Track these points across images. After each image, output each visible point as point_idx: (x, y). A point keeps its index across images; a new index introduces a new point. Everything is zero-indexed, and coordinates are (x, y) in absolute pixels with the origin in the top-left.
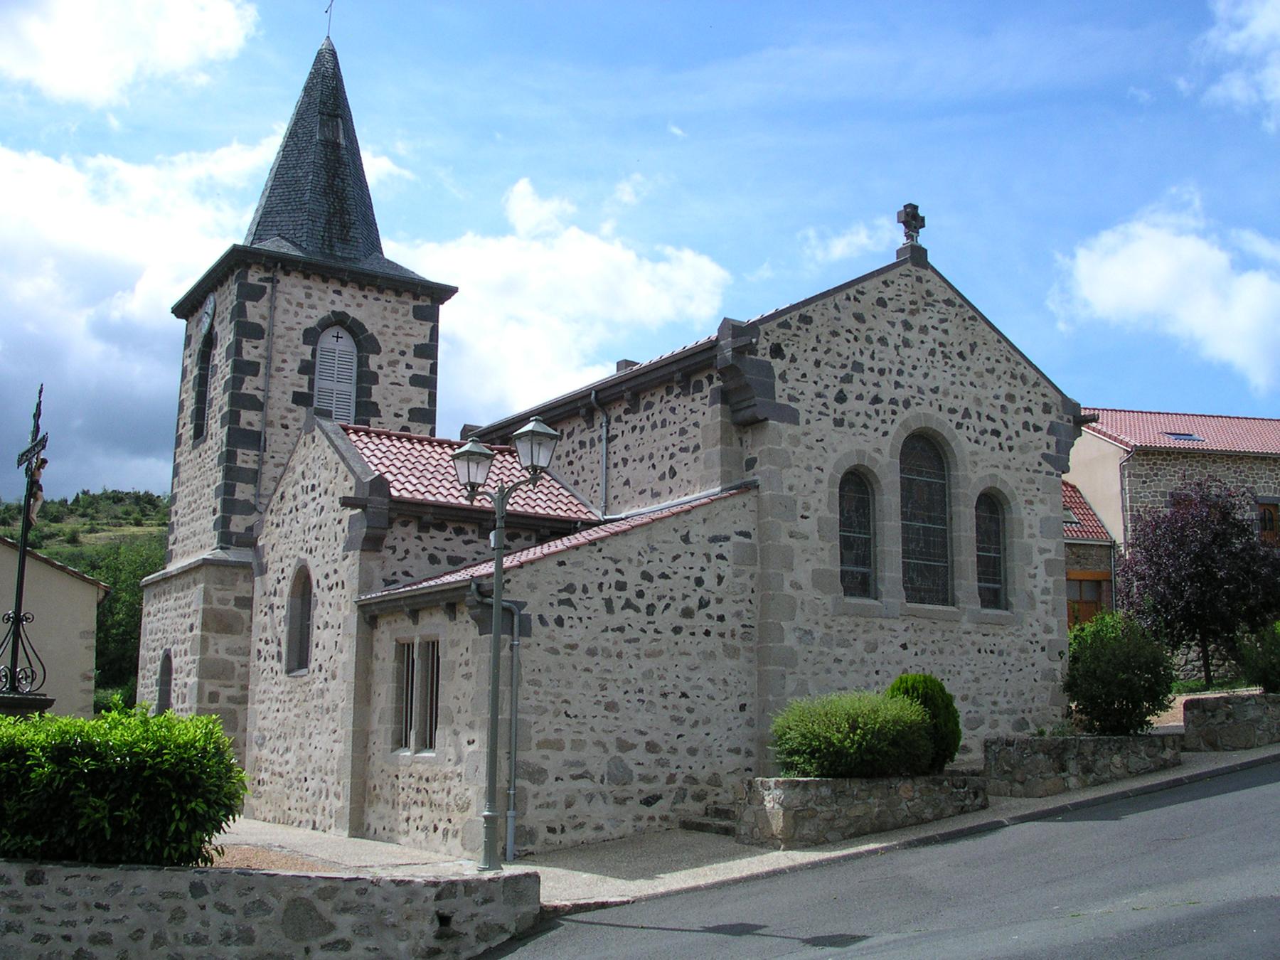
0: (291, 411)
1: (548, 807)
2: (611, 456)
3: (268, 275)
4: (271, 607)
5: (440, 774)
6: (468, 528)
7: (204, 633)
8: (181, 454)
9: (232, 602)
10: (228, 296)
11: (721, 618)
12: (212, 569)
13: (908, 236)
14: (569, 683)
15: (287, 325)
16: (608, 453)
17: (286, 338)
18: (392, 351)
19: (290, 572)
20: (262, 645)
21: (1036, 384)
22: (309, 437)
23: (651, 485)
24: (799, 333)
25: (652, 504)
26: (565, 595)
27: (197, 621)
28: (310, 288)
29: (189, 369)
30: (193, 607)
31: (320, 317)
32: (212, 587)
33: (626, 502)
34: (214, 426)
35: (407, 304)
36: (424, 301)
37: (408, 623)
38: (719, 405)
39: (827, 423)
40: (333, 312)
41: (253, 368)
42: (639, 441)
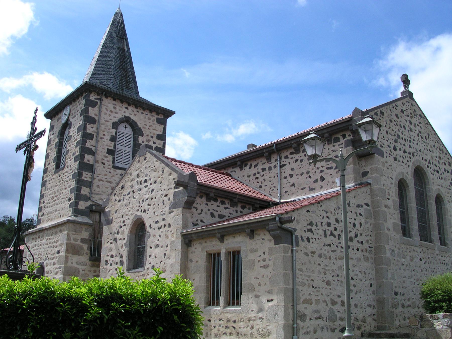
0: (106, 157)
1: (307, 334)
2: (283, 174)
3: (98, 97)
4: (115, 240)
5: (245, 318)
6: (226, 202)
7: (67, 254)
8: (47, 177)
9: (80, 241)
10: (81, 104)
11: (362, 243)
12: (71, 225)
13: (405, 87)
14: (313, 271)
15: (106, 120)
16: (281, 172)
17: (105, 125)
18: (148, 135)
19: (129, 222)
20: (109, 258)
21: (446, 154)
22: (142, 158)
23: (309, 185)
24: (381, 118)
25: (310, 194)
26: (309, 227)
27: (63, 249)
28: (115, 105)
29: (52, 140)
30: (59, 243)
31: (119, 118)
32: (71, 233)
33: (293, 194)
34: (69, 162)
35: (154, 117)
36: (161, 116)
37: (218, 243)
38: (351, 147)
39: (392, 159)
40: (125, 116)
41: (90, 136)
42: (300, 166)
